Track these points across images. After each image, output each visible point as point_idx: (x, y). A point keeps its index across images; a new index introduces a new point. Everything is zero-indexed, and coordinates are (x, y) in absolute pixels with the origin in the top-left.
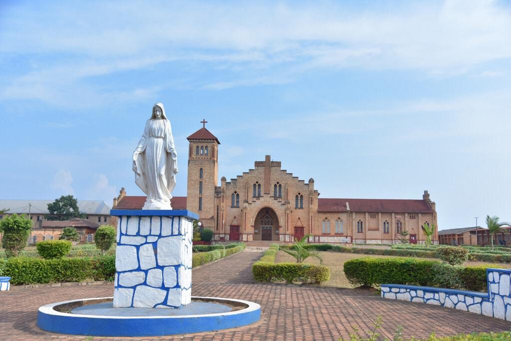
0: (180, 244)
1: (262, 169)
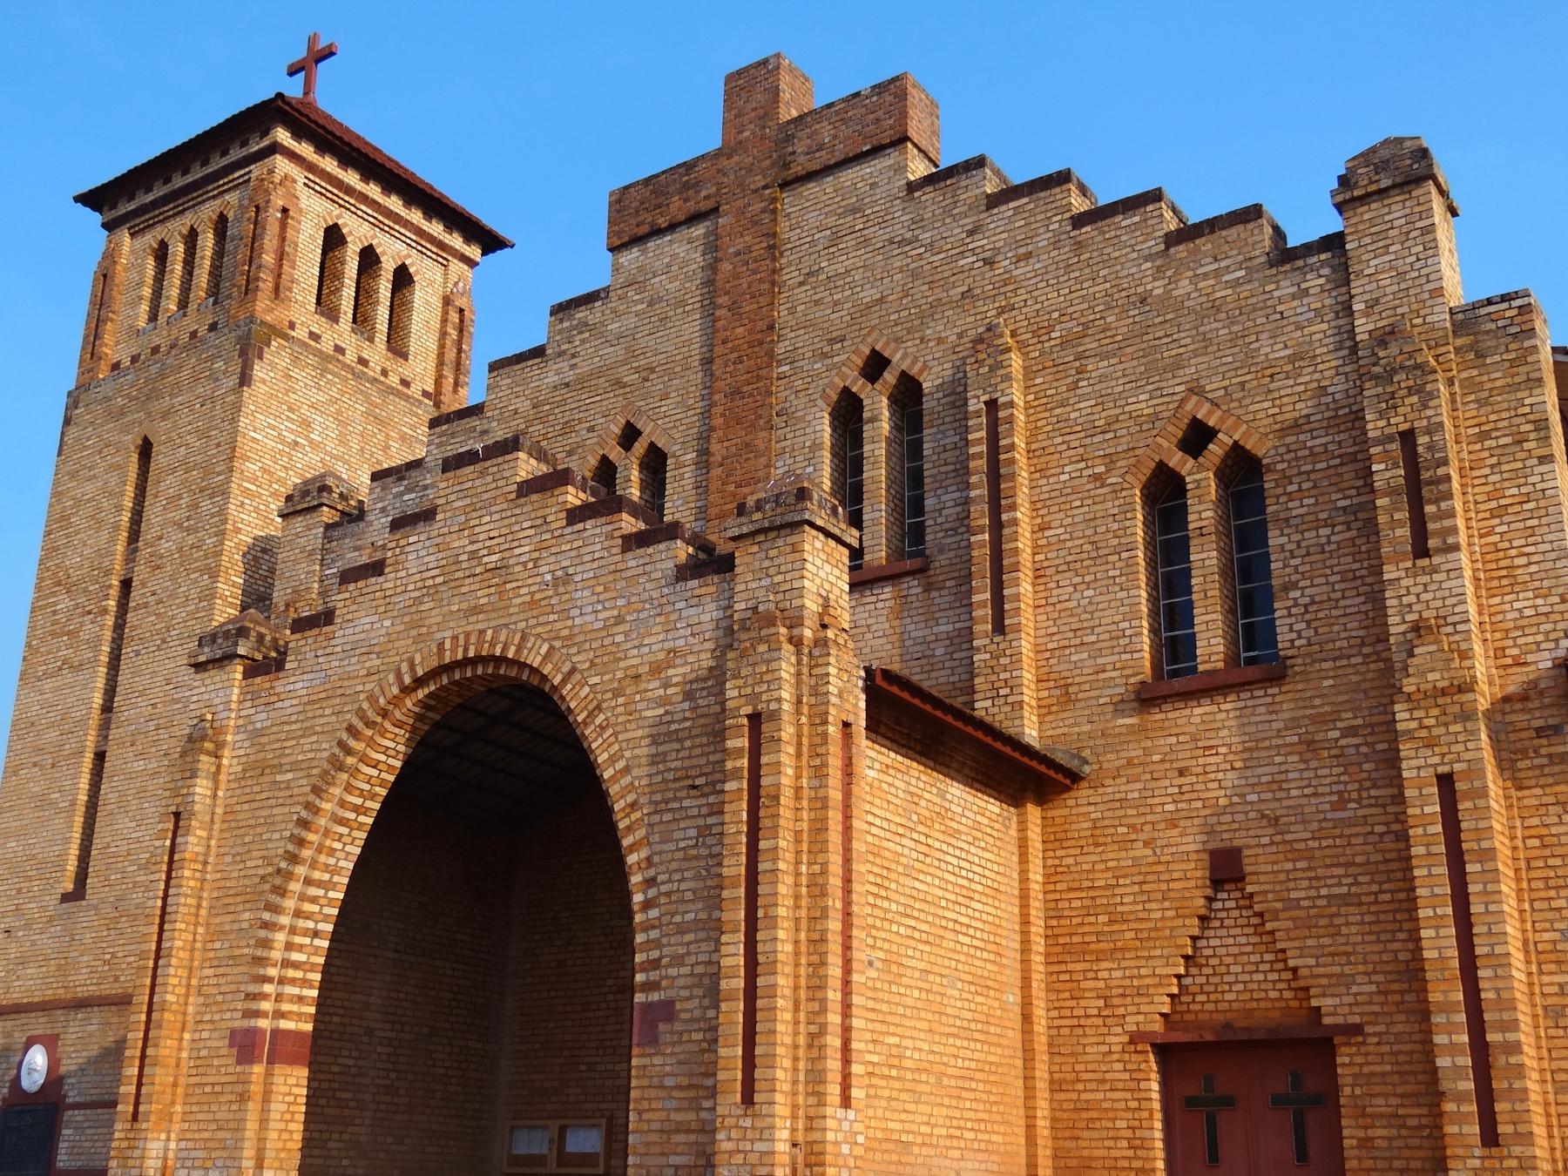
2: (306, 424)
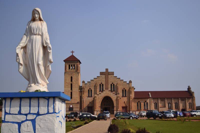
0: (54, 120)
1: (104, 76)
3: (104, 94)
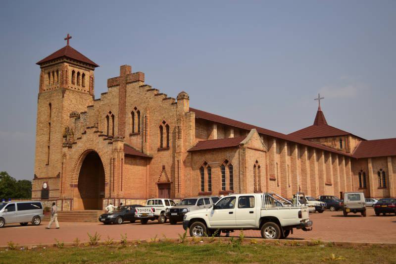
1: (116, 90)
2: (72, 101)
3: (81, 147)
